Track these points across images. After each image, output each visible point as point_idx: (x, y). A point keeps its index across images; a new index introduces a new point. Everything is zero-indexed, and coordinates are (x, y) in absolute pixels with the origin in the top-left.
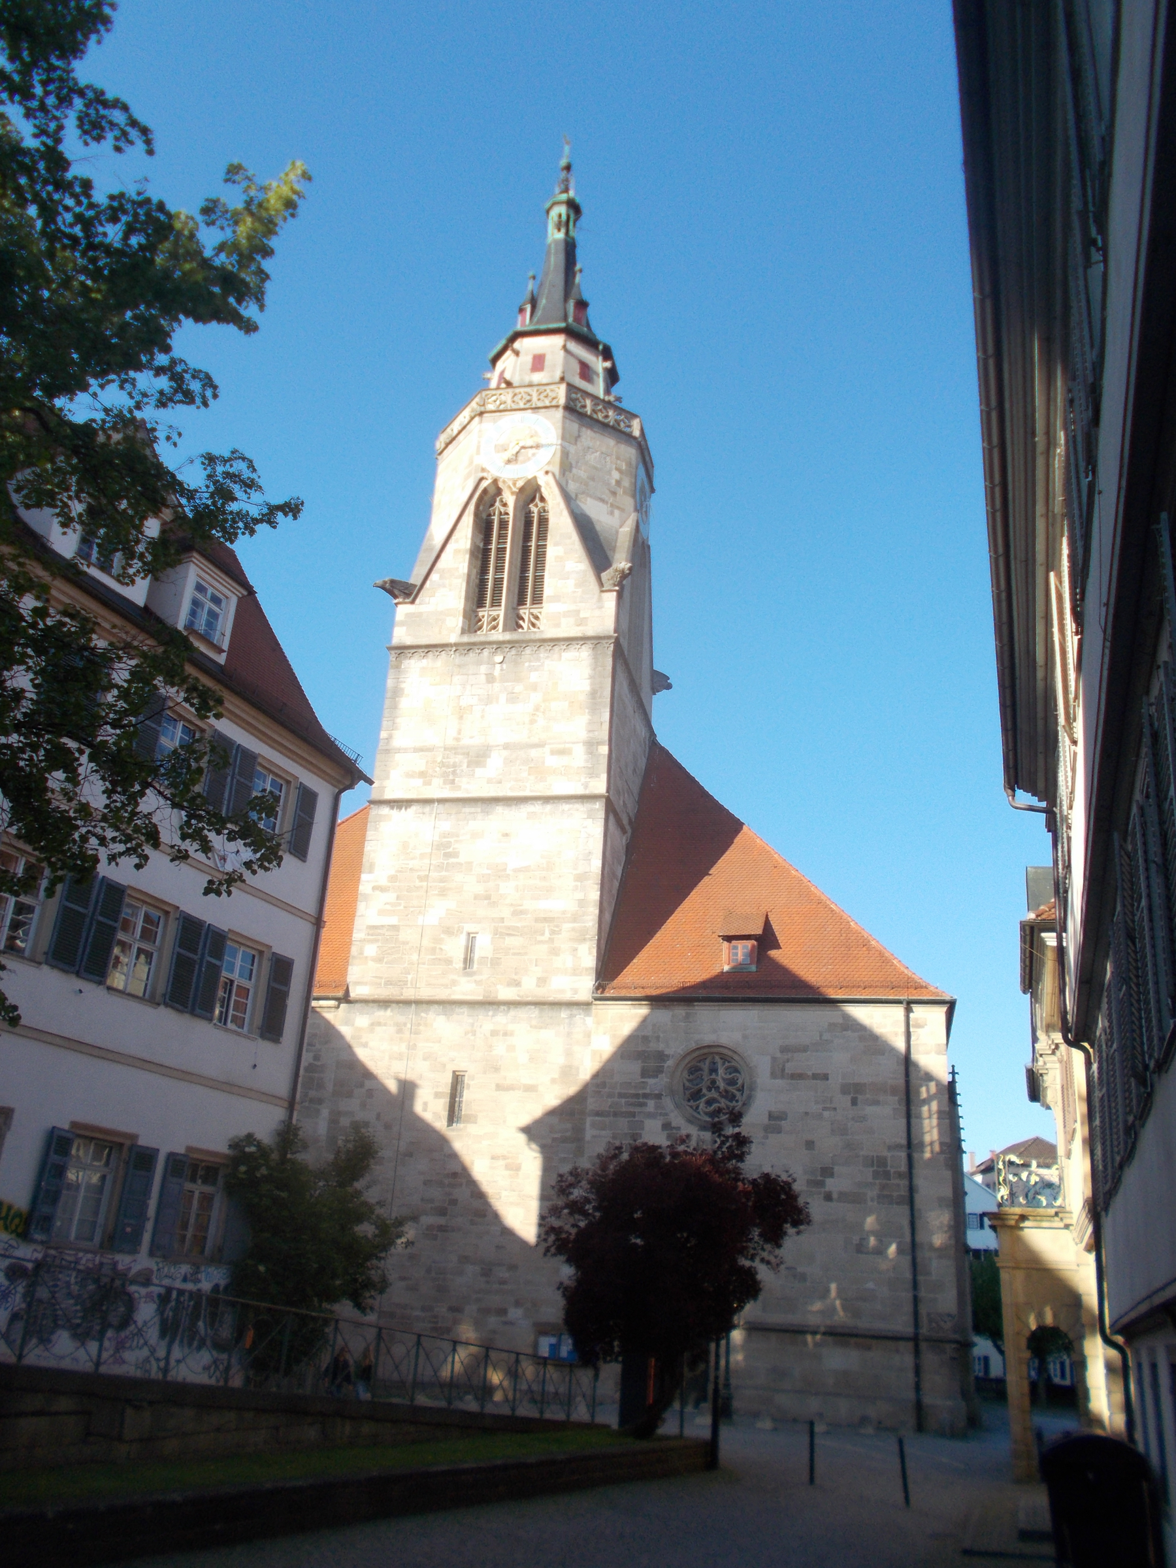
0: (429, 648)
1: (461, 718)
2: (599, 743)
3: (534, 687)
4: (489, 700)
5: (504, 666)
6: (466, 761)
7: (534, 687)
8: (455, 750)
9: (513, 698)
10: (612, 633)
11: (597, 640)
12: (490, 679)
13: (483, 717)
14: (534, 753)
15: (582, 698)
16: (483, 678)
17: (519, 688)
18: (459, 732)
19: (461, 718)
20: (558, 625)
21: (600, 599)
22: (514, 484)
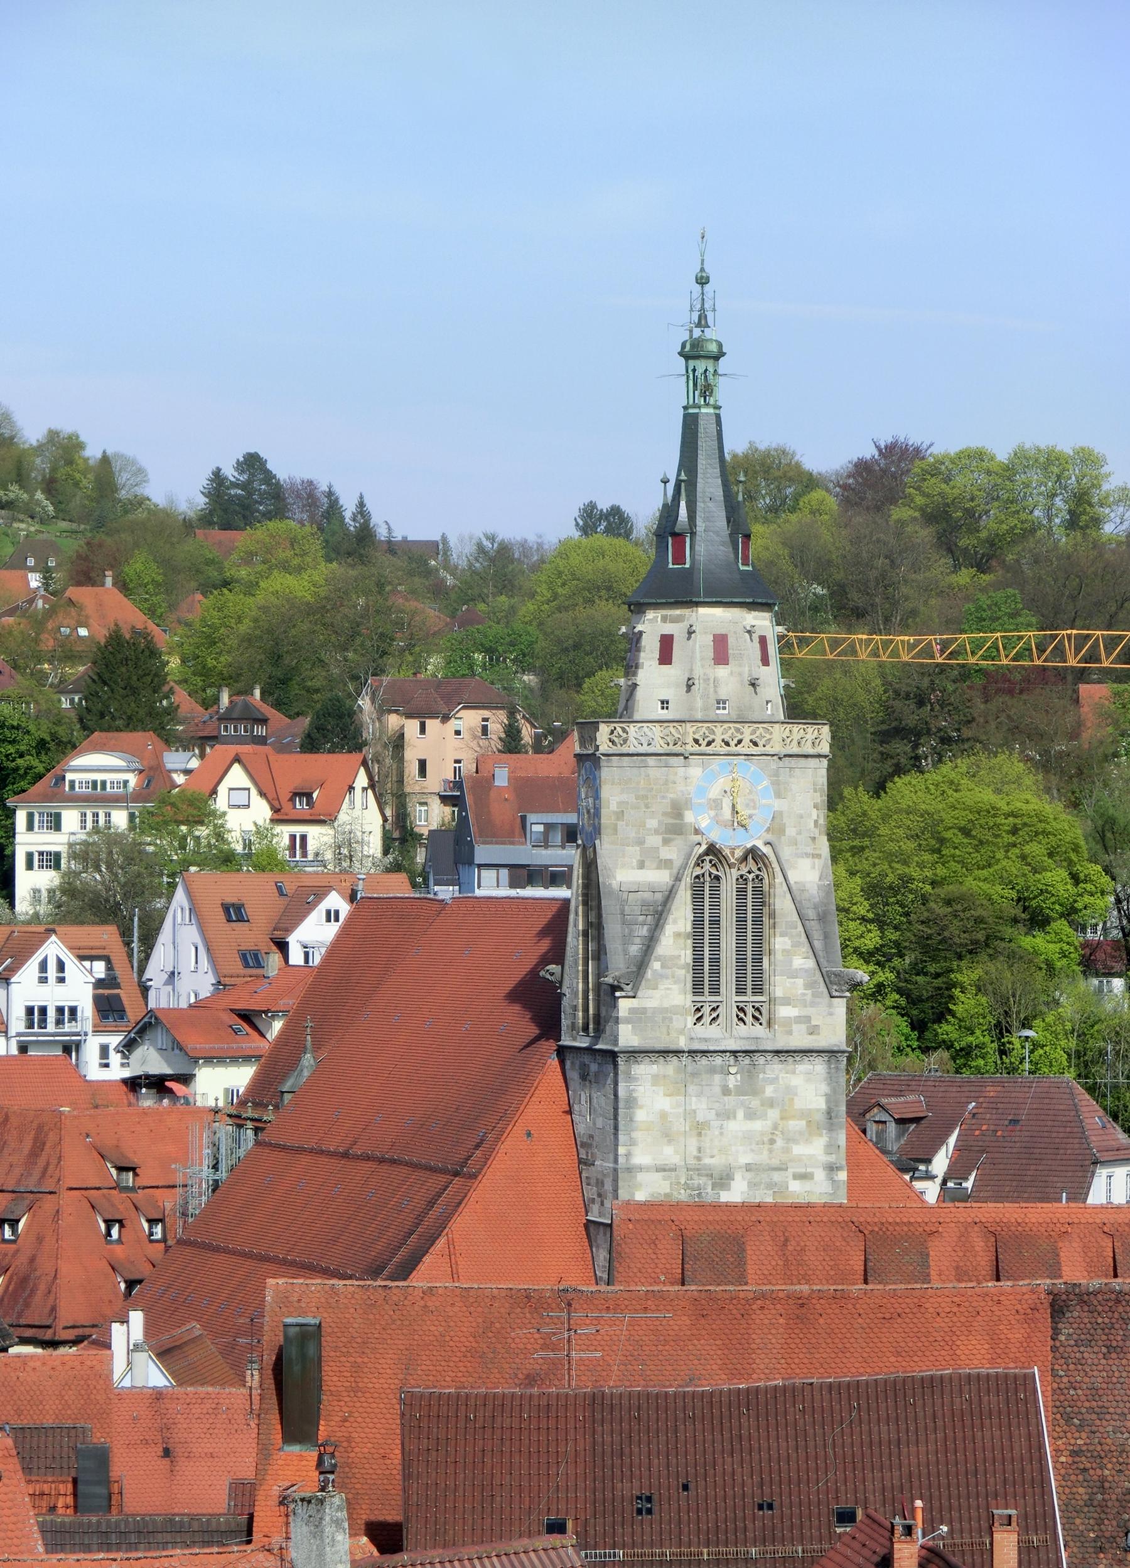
0: (665, 1053)
1: (700, 1134)
2: (838, 1169)
3: (771, 1103)
4: (727, 1115)
5: (738, 1076)
6: (710, 1182)
7: (771, 1103)
8: (698, 1170)
9: (751, 1115)
10: (844, 1047)
11: (831, 1053)
12: (726, 1091)
13: (721, 1134)
14: (777, 1177)
15: (820, 1117)
16: (717, 1090)
17: (755, 1103)
18: (699, 1150)
19: (700, 1134)
20: (790, 1033)
21: (830, 1006)
22: (733, 854)
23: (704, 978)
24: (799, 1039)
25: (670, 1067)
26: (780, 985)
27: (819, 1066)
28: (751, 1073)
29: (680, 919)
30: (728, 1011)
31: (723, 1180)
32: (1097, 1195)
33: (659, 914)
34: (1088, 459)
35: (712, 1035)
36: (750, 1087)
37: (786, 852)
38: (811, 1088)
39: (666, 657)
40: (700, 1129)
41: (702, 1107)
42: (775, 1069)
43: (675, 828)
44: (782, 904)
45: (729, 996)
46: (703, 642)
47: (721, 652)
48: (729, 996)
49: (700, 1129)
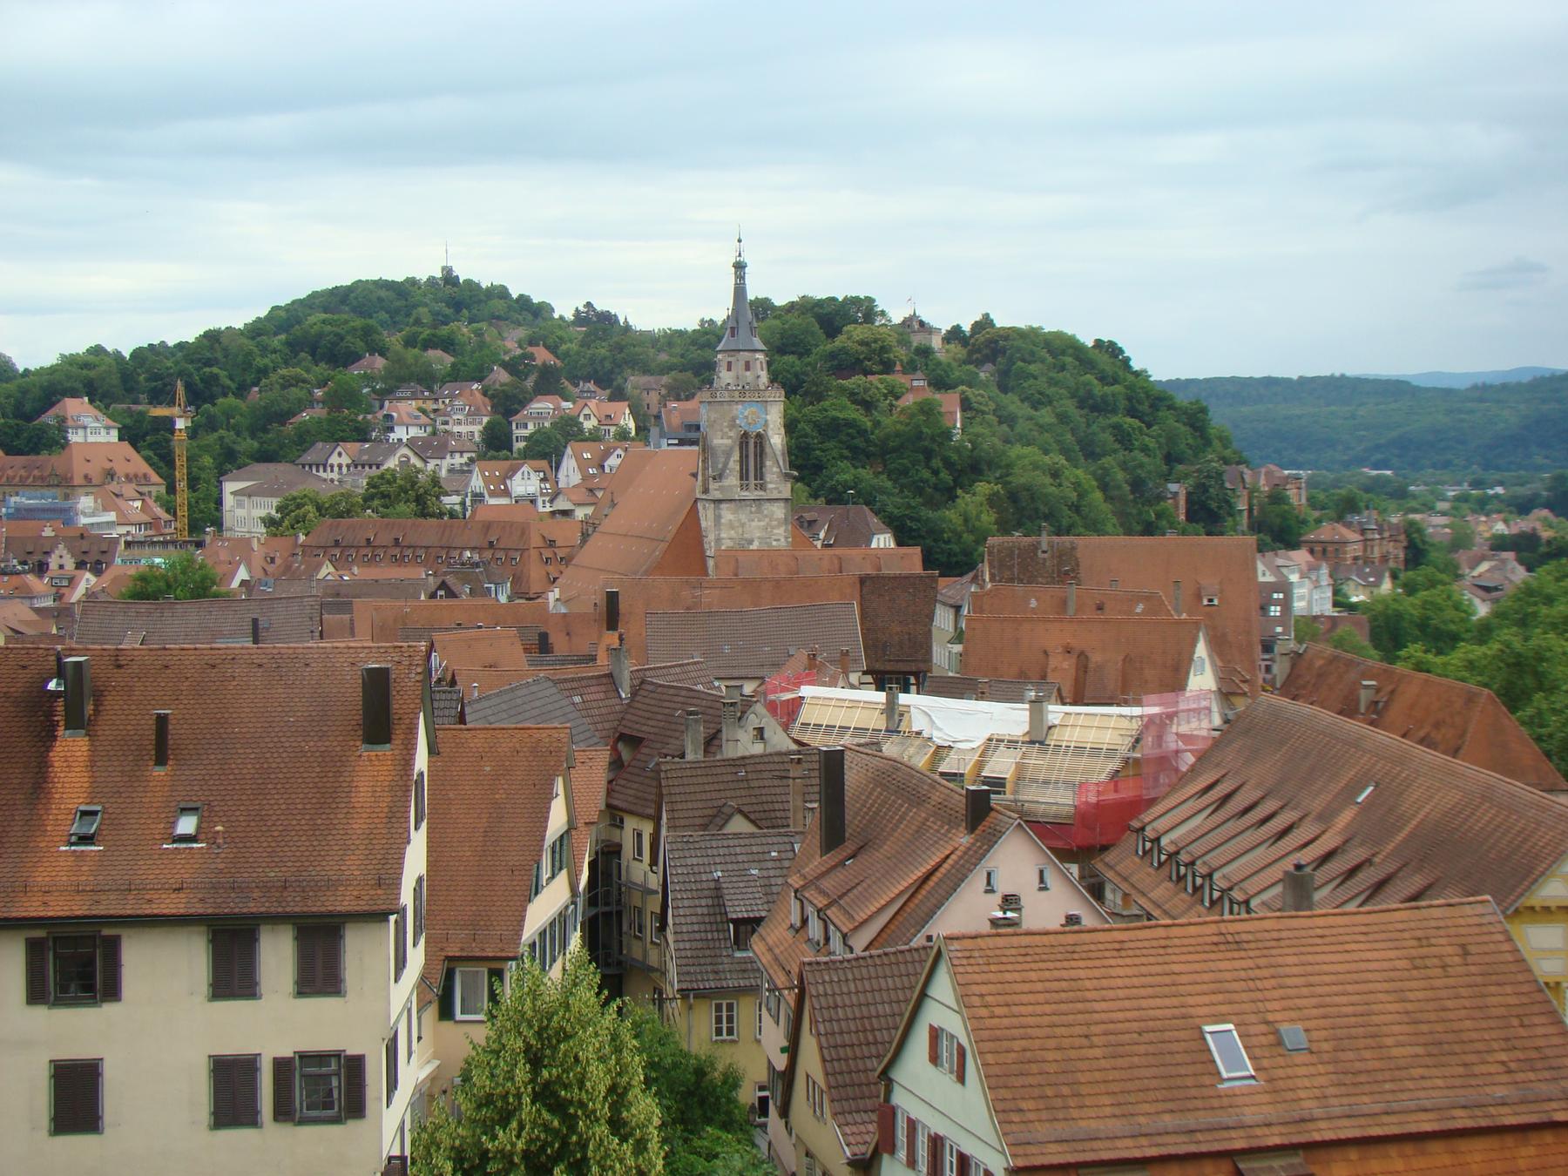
23: (744, 476)
24: (775, 495)
25: (732, 505)
26: (768, 477)
27: (782, 504)
28: (759, 507)
29: (736, 456)
30: (752, 486)
31: (751, 542)
32: (874, 545)
33: (728, 455)
34: (870, 300)
35: (745, 494)
36: (759, 511)
37: (770, 433)
38: (779, 511)
39: (729, 369)
40: (743, 525)
41: (743, 518)
42: (767, 505)
43: (733, 425)
44: (768, 450)
45: (752, 481)
46: (742, 364)
47: (748, 367)
48: (752, 481)
49: (743, 525)
